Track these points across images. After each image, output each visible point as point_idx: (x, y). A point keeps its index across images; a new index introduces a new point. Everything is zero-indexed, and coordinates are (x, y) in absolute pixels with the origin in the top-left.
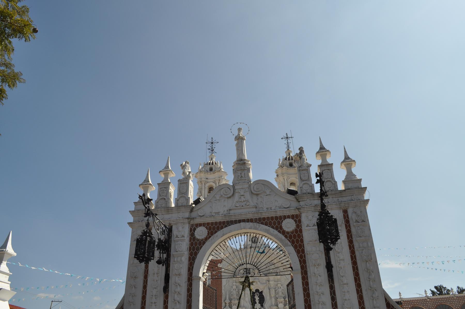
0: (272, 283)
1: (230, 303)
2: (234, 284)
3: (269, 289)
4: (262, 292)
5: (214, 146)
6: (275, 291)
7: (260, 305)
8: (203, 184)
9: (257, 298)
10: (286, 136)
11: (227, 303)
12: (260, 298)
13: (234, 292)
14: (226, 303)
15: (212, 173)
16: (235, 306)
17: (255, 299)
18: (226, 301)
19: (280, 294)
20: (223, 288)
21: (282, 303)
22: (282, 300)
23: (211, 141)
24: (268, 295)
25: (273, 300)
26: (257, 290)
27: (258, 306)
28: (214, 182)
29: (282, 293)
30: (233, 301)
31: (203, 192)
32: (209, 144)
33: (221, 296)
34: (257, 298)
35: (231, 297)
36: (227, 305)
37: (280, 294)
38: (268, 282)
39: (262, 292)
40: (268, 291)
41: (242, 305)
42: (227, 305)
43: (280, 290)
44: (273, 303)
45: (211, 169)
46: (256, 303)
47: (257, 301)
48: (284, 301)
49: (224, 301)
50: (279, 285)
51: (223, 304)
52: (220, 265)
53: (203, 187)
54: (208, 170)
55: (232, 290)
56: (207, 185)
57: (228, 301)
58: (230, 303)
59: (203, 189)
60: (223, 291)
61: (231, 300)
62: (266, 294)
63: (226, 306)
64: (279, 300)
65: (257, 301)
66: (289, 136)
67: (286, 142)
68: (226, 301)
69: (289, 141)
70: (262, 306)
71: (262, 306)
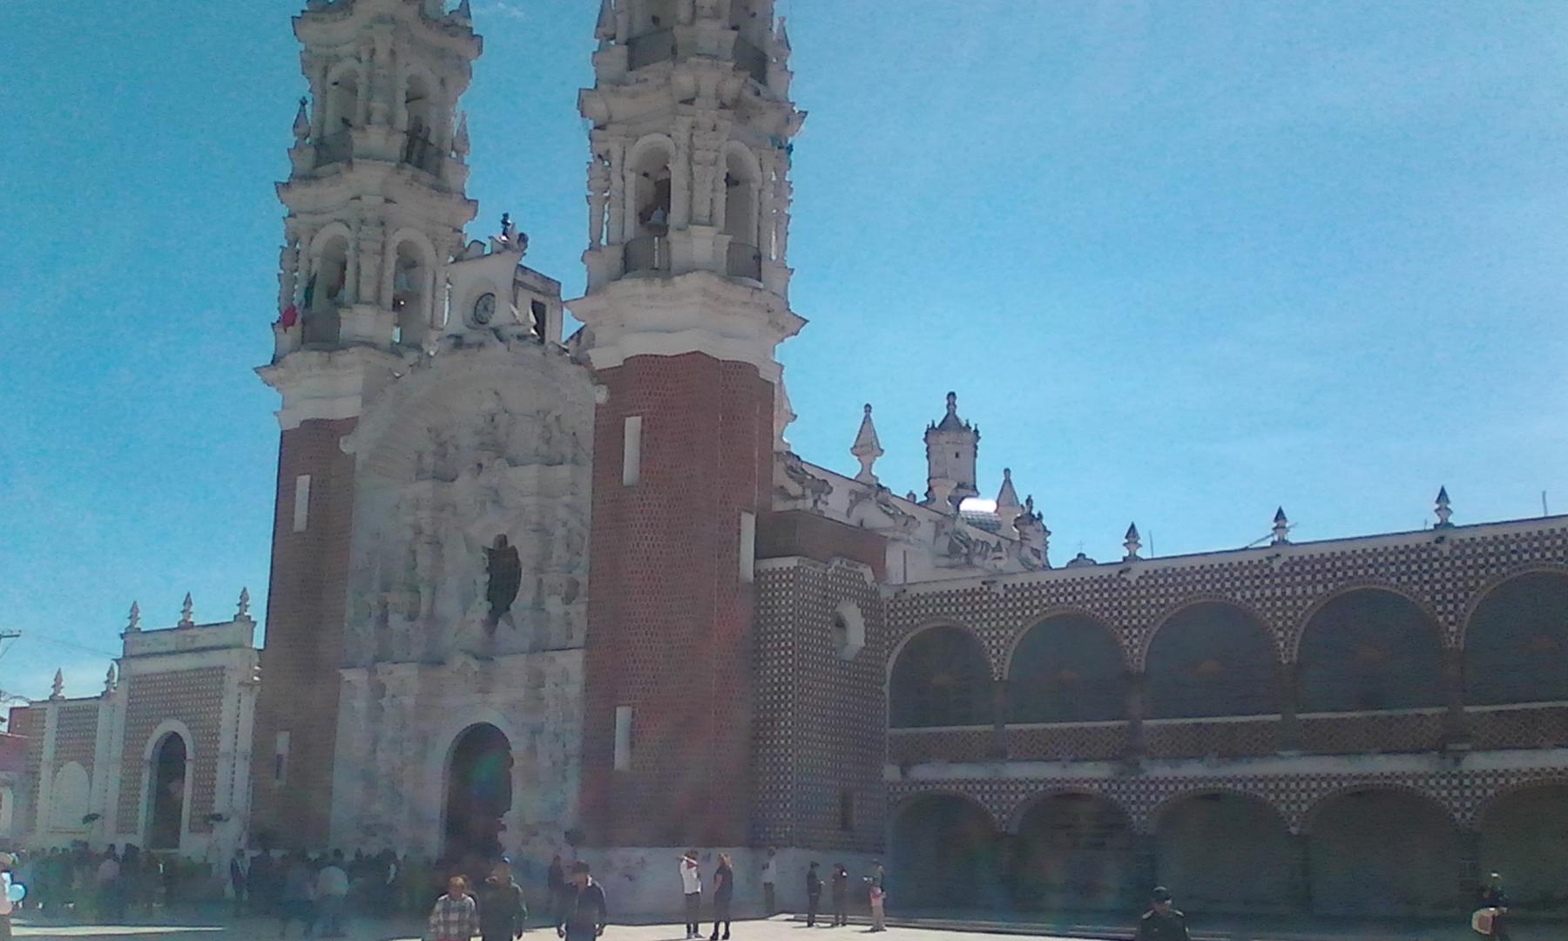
7: (487, 605)
41: (424, 609)
52: (347, 446)
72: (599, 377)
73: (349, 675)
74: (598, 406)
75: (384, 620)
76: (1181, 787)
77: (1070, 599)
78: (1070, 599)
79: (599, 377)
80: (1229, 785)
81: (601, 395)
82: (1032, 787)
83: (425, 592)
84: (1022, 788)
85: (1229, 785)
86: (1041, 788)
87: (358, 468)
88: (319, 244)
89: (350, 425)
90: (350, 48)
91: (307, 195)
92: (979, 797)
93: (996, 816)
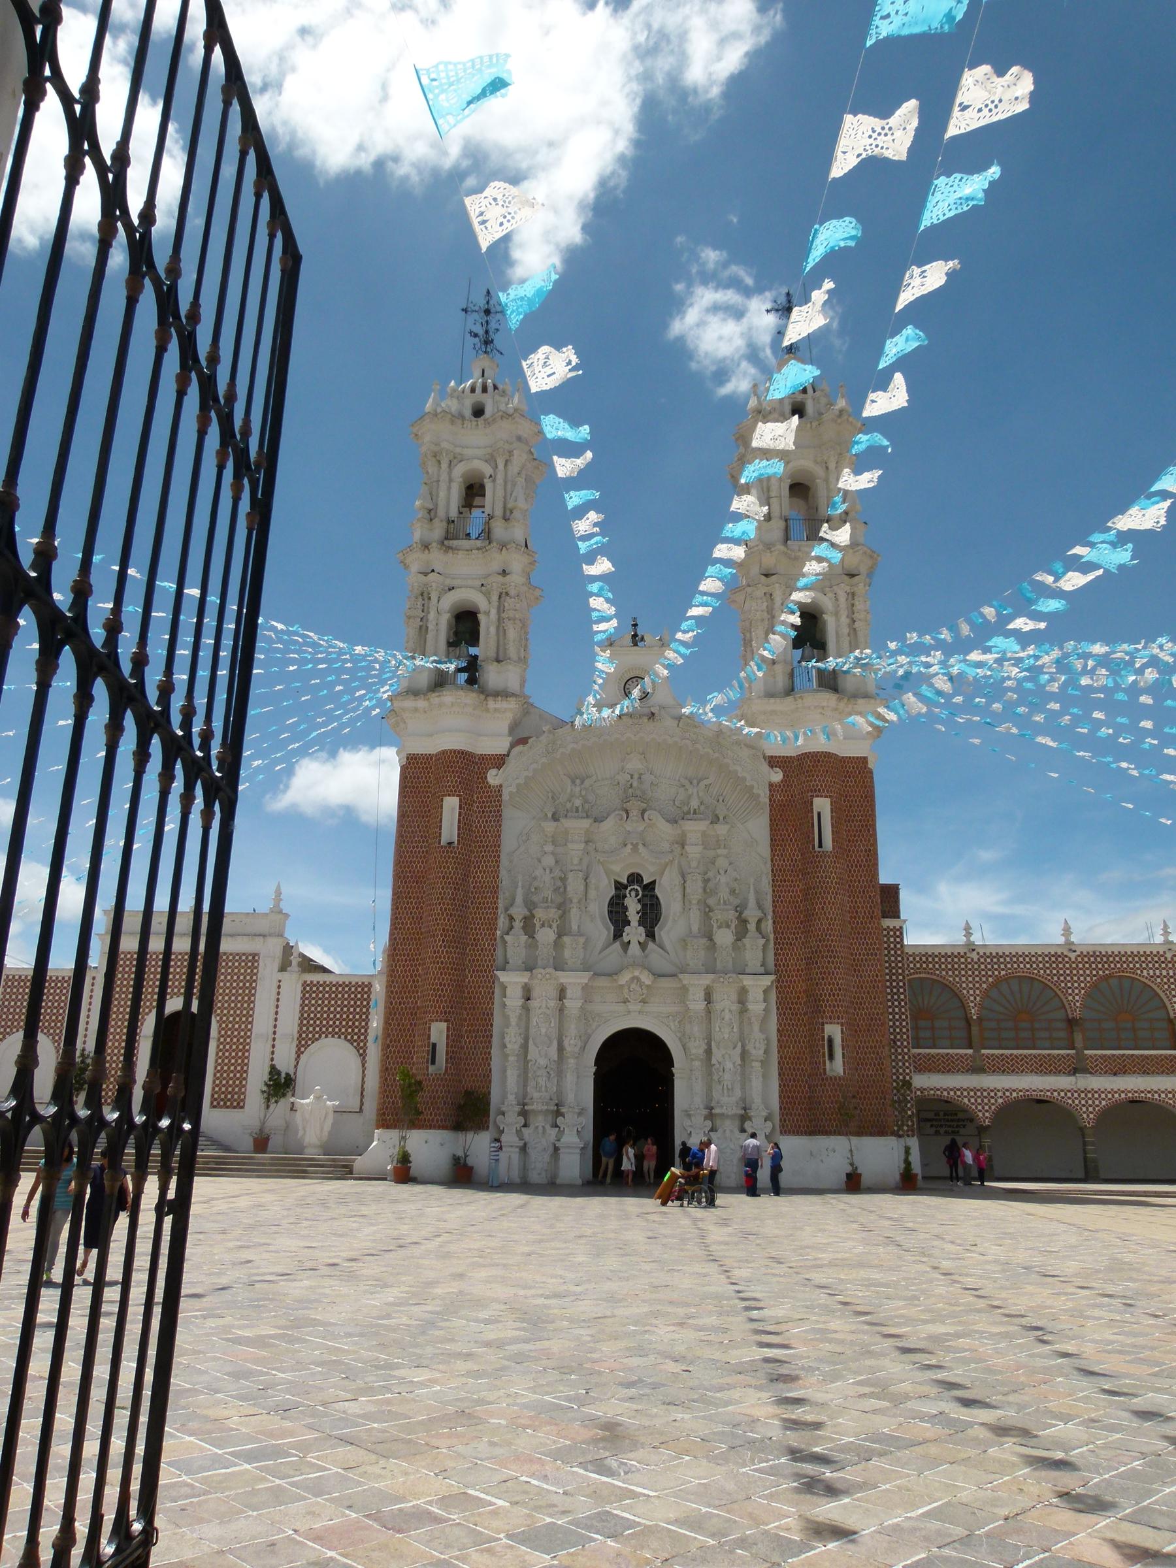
2: (549, 848)
3: (683, 877)
5: (493, 325)
6: (706, 881)
7: (641, 930)
8: (444, 465)
9: (633, 906)
12: (644, 906)
13: (547, 878)
14: (511, 918)
15: (481, 420)
17: (626, 909)
18: (512, 911)
19: (724, 894)
20: (504, 861)
21: (728, 926)
23: (481, 302)
24: (679, 895)
25: (695, 915)
26: (635, 878)
27: (634, 932)
28: (491, 460)
29: (733, 892)
30: (540, 914)
31: (442, 494)
32: (475, 316)
33: (495, 891)
34: (633, 906)
35: (535, 898)
36: (518, 924)
39: (654, 882)
40: (677, 880)
41: (575, 927)
42: (518, 924)
43: (723, 879)
45: (478, 412)
46: (629, 923)
48: (735, 923)
49: (507, 909)
50: (722, 863)
51: (502, 921)
52: (493, 777)
53: (444, 477)
54: (468, 412)
55: (538, 872)
56: (459, 470)
57: (519, 911)
59: (443, 486)
60: (503, 873)
61: (530, 905)
62: (667, 893)
63: (511, 928)
64: (717, 915)
68: (512, 911)
70: (651, 935)
71: (651, 935)
72: (774, 762)
73: (503, 977)
74: (771, 785)
76: (1116, 1095)
77: (1028, 966)
78: (1028, 966)
80: (1149, 1095)
81: (777, 776)
82: (1008, 1094)
83: (574, 913)
84: (1000, 1094)
85: (1149, 1095)
86: (1015, 1094)
88: (449, 602)
89: (499, 761)
90: (480, 452)
91: (437, 558)
92: (966, 1100)
93: (980, 1114)
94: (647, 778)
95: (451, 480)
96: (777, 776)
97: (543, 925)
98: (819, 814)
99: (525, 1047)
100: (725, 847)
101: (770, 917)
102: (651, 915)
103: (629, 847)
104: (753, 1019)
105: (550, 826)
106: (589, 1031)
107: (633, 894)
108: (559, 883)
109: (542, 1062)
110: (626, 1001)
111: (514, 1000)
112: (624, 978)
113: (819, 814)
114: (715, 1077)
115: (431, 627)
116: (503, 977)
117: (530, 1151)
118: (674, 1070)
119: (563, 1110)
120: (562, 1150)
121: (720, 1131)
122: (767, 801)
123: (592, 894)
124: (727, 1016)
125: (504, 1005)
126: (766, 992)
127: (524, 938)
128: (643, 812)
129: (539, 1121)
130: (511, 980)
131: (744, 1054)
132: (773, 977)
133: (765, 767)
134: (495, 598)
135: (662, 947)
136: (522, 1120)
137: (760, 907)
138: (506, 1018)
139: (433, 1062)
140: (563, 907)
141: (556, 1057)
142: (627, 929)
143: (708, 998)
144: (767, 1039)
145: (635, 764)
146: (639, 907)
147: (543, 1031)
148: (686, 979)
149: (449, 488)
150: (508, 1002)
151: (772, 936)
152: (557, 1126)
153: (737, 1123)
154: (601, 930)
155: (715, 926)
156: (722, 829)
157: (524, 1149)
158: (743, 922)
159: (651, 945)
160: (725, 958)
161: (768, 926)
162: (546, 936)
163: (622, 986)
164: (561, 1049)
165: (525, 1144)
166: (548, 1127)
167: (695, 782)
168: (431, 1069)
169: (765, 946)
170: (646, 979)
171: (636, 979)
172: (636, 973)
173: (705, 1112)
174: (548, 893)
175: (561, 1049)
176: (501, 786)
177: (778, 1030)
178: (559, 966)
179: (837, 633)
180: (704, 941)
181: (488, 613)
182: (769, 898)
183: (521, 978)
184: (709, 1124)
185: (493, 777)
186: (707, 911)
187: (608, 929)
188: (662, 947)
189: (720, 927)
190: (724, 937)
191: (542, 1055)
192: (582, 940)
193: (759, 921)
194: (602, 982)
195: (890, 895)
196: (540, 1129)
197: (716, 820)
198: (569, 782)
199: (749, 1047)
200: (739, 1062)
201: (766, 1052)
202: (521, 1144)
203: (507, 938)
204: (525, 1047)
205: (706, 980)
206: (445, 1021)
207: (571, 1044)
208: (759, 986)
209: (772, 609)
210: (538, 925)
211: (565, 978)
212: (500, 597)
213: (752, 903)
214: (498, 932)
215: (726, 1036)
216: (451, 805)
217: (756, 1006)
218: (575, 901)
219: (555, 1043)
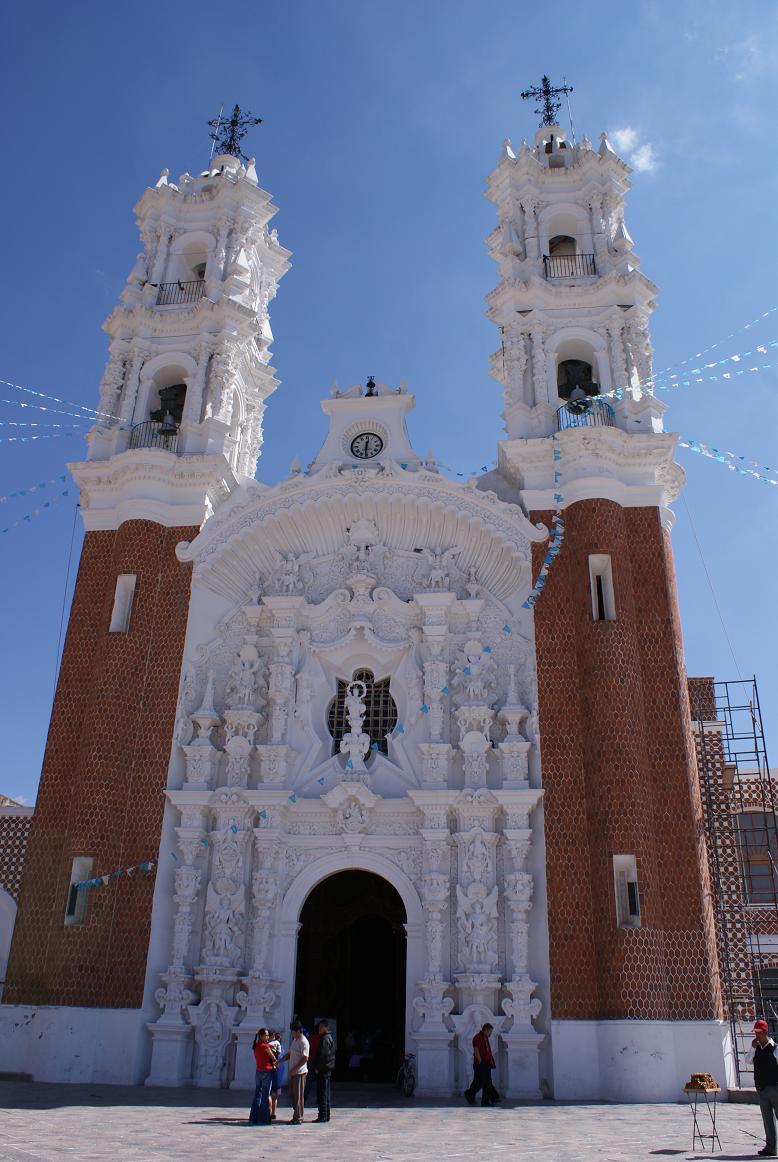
0: (435, 633)
1: (218, 727)
2: (253, 638)
4: (387, 683)
7: (366, 738)
10: (540, 85)
11: (205, 723)
13: (247, 676)
14: (196, 726)
16: (239, 739)
18: (198, 716)
19: (476, 686)
21: (481, 729)
22: (483, 713)
23: (230, 116)
24: (415, 692)
25: (436, 714)
26: (364, 675)
27: (357, 742)
29: (487, 685)
34: (356, 707)
36: (205, 733)
37: (476, 686)
38: (414, 634)
39: (387, 683)
41: (277, 734)
43: (475, 669)
44: (436, 730)
46: (348, 730)
47: (356, 722)
51: (180, 728)
52: (183, 552)
57: (206, 717)
58: (218, 727)
61: (220, 708)
62: (402, 694)
63: (195, 736)
64: (465, 713)
65: (356, 722)
66: (554, 84)
67: (541, 105)
68: (197, 716)
69: (553, 101)
72: (536, 517)
75: (218, 742)
79: (536, 517)
81: (540, 533)
87: (195, 576)
88: (151, 368)
89: (191, 533)
94: (378, 549)
95: (169, 254)
96: (540, 533)
97: (236, 733)
98: (599, 580)
99: (201, 894)
100: (478, 630)
101: (535, 713)
102: (381, 720)
103: (353, 632)
104: (514, 853)
105: (253, 612)
106: (293, 874)
107: (356, 691)
108: (262, 682)
109: (224, 915)
110: (341, 832)
111: (190, 832)
112: (335, 798)
113: (599, 580)
114: (461, 936)
115: (130, 391)
116: (174, 797)
117: (198, 1037)
118: (406, 927)
119: (245, 980)
120: (157, 1036)
121: (466, 1013)
122: (530, 565)
123: (304, 693)
124: (479, 849)
125: (176, 838)
126: (531, 815)
127: (208, 749)
128: (373, 589)
129: (214, 997)
130: (186, 802)
131: (502, 901)
132: (541, 792)
133: (527, 522)
134: (204, 359)
135: (394, 762)
136: (191, 996)
137: (524, 702)
138: (178, 855)
139: (71, 912)
140: (265, 712)
141: (242, 908)
142: (346, 737)
143: (454, 826)
144: (534, 880)
145: (363, 533)
146: (363, 708)
147: (228, 872)
148: (419, 798)
149: (167, 260)
150: (182, 832)
151: (538, 737)
152: (234, 1004)
153: (492, 1000)
154: (311, 735)
155: (463, 729)
156: (473, 606)
157: (191, 1035)
158: (500, 723)
159: (379, 757)
160: (476, 768)
161: (534, 722)
162: (237, 746)
163: (335, 811)
164: (250, 896)
165: (194, 1029)
166: (223, 1005)
167: (438, 551)
168: (68, 921)
169: (530, 754)
170: (368, 800)
171: (353, 800)
172: (352, 791)
173: (445, 986)
174: (245, 692)
175: (250, 896)
176: (192, 562)
177: (548, 866)
178: (253, 783)
179: (612, 372)
180: (448, 746)
181: (194, 376)
182: (534, 689)
183: (202, 798)
184: (450, 1003)
185: (183, 552)
186: (451, 711)
187: (323, 739)
188: (394, 762)
189: (469, 730)
190: (474, 743)
191: (224, 903)
192: (283, 750)
193: (522, 722)
194: (305, 807)
195: (703, 689)
196: (214, 1009)
197: (465, 595)
198: (278, 557)
199: (508, 893)
200: (495, 913)
201: (532, 899)
202: (186, 1029)
203: (187, 749)
204: (201, 894)
205: (450, 797)
206: (91, 855)
207: (267, 890)
208: (523, 801)
209: (531, 348)
210: (229, 734)
211: (257, 799)
212: (211, 357)
213: (512, 696)
214: (174, 741)
215: (477, 877)
216: (126, 583)
217: (518, 837)
218: (280, 701)
219: (242, 889)
